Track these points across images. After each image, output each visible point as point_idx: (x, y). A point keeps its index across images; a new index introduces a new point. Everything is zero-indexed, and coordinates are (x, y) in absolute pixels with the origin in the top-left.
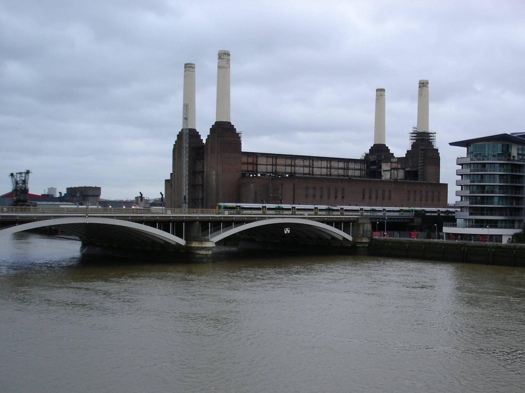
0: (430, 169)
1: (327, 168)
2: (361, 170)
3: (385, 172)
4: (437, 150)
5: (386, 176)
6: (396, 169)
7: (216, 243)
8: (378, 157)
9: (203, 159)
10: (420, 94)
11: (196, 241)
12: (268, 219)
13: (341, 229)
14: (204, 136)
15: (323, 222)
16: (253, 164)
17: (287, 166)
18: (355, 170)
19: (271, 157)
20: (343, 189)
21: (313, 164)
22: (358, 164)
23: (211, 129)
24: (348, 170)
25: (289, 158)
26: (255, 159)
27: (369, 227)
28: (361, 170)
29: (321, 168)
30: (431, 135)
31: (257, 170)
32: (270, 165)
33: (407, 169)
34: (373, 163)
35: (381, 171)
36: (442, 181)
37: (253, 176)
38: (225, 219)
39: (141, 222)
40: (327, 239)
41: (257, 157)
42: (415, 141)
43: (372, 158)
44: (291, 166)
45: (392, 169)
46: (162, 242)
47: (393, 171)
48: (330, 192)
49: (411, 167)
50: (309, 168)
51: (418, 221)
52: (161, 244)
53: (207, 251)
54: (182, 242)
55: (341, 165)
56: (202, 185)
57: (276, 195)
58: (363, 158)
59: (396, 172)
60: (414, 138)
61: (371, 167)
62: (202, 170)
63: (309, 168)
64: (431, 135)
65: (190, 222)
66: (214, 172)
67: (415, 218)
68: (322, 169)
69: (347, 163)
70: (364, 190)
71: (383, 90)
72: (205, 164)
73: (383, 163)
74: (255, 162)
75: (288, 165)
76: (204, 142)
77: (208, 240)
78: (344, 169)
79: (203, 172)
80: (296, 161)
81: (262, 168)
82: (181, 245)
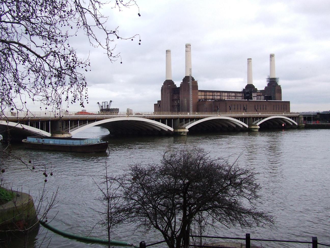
0: (277, 95)
1: (228, 96)
2: (242, 96)
3: (254, 97)
4: (280, 86)
5: (255, 99)
6: (260, 95)
7: (260, 125)
8: (250, 90)
10: (271, 60)
13: (294, 120)
22: (240, 94)
25: (211, 92)
27: (302, 119)
28: (242, 96)
29: (224, 96)
30: (276, 79)
32: (202, 95)
33: (266, 96)
34: (248, 93)
35: (252, 97)
36: (283, 100)
38: (256, 116)
39: (235, 118)
42: (269, 82)
43: (247, 91)
44: (213, 96)
45: (257, 96)
46: (235, 126)
47: (258, 97)
49: (268, 95)
51: (318, 116)
55: (233, 94)
58: (242, 91)
59: (260, 97)
60: (269, 81)
61: (247, 95)
64: (276, 79)
65: (249, 118)
66: (186, 100)
67: (318, 115)
68: (225, 97)
70: (255, 105)
71: (251, 59)
72: (180, 96)
73: (253, 93)
75: (211, 96)
78: (235, 96)
82: (246, 127)
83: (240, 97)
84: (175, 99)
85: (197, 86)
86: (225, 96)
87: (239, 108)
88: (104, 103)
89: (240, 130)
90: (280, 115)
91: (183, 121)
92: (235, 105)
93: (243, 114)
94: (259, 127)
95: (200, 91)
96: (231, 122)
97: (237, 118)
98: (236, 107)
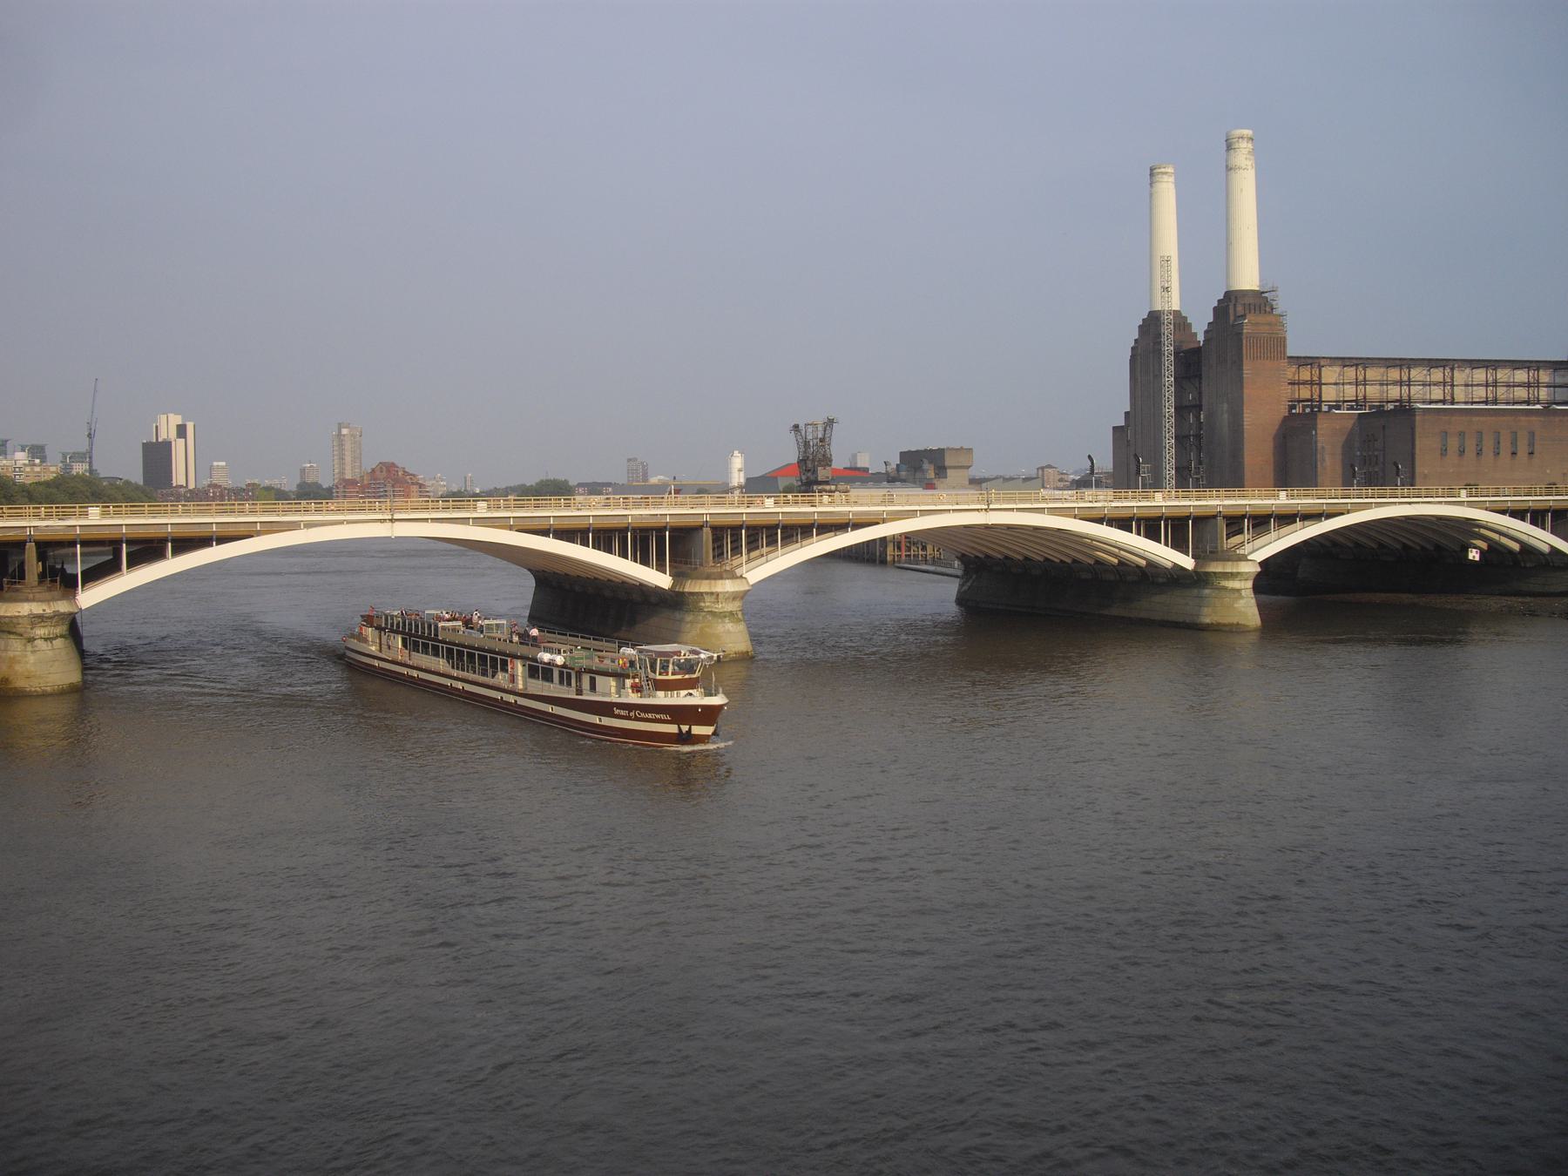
7: (1262, 564)
9: (1200, 377)
11: (1217, 560)
12: (1376, 507)
14: (1200, 324)
15: (1503, 512)
16: (1311, 383)
17: (1390, 384)
18: (1555, 387)
19: (1352, 366)
20: (1532, 434)
21: (1452, 378)
23: (1215, 309)
24: (1538, 387)
26: (1316, 371)
31: (1320, 396)
32: (1350, 383)
37: (1312, 411)
40: (1510, 551)
41: (1320, 367)
44: (1400, 383)
48: (1499, 443)
50: (1442, 388)
52: (1138, 567)
53: (1243, 582)
54: (1187, 562)
56: (1198, 437)
57: (1370, 453)
62: (1198, 403)
63: (1444, 386)
65: (1202, 520)
66: (1225, 406)
69: (1534, 370)
74: (1315, 378)
75: (1395, 383)
76: (1201, 338)
77: (1244, 558)
78: (1528, 385)
79: (1200, 407)
80: (1414, 372)
81: (1329, 394)
83: (1556, 389)
84: (1187, 404)
85: (1282, 342)
86: (1478, 385)
87: (1488, 444)
88: (810, 429)
89: (1165, 580)
90: (1440, 503)
91: (797, 535)
92: (1462, 434)
93: (1163, 501)
94: (1259, 569)
95: (1340, 362)
96: (1078, 536)
97: (1123, 523)
98: (1470, 446)
